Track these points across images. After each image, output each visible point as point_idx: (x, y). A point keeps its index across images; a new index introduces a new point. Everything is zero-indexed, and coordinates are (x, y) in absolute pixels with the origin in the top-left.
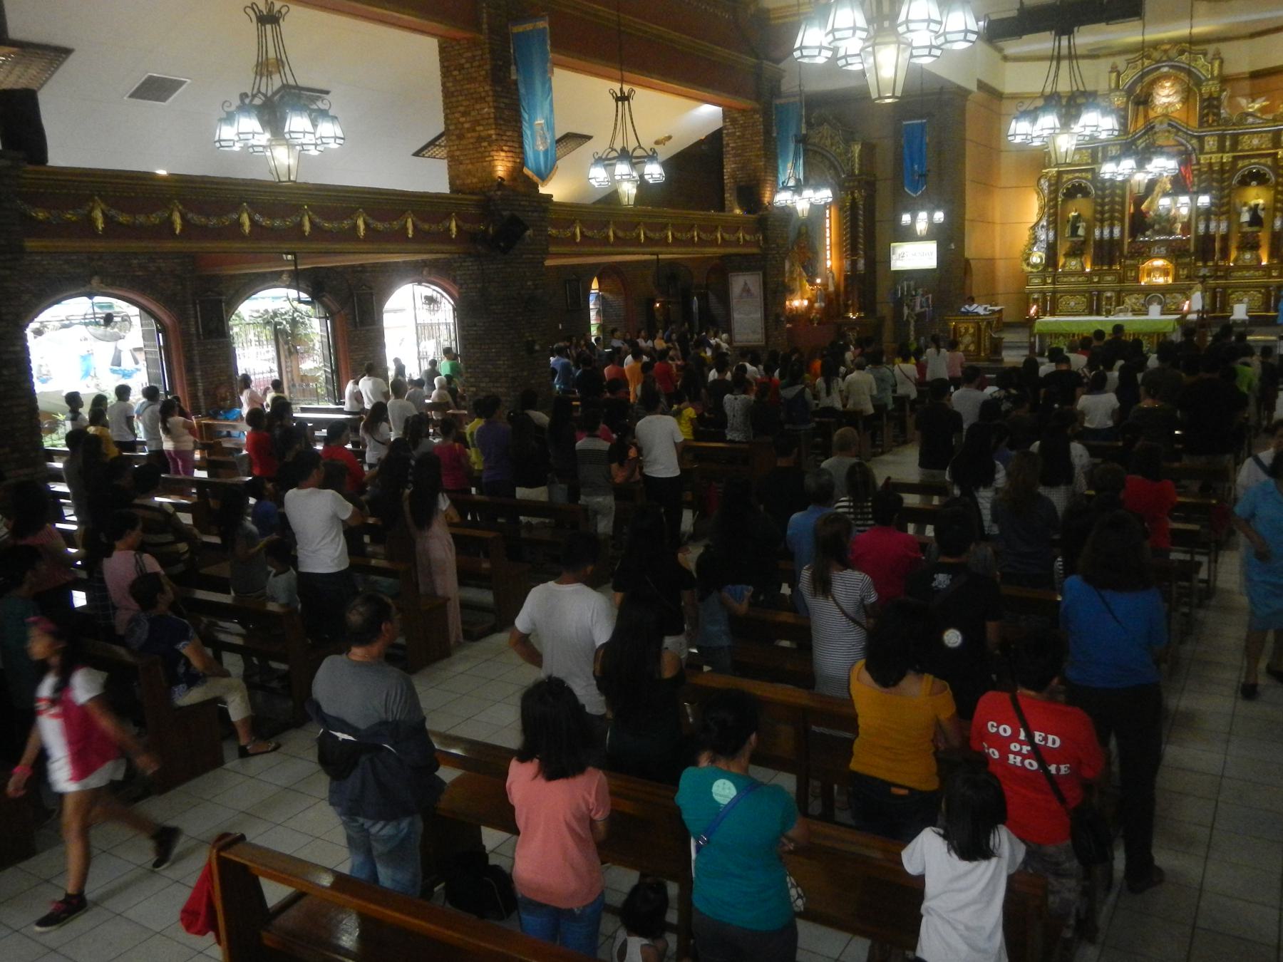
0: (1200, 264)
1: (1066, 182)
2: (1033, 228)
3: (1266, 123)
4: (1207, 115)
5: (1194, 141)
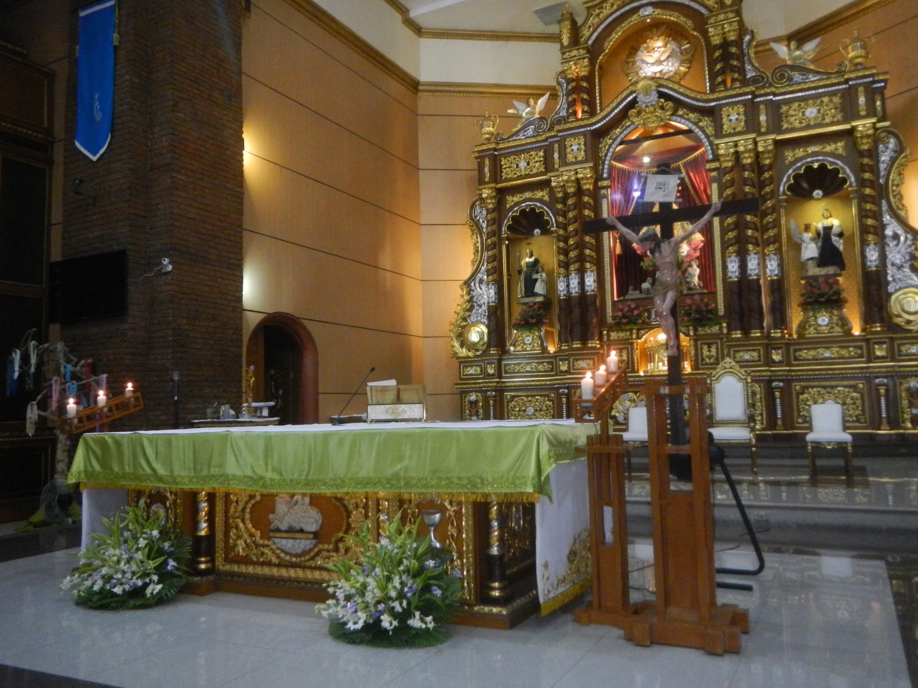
0: (738, 335)
1: (512, 208)
2: (467, 283)
3: (827, 79)
4: (723, 71)
5: (706, 122)
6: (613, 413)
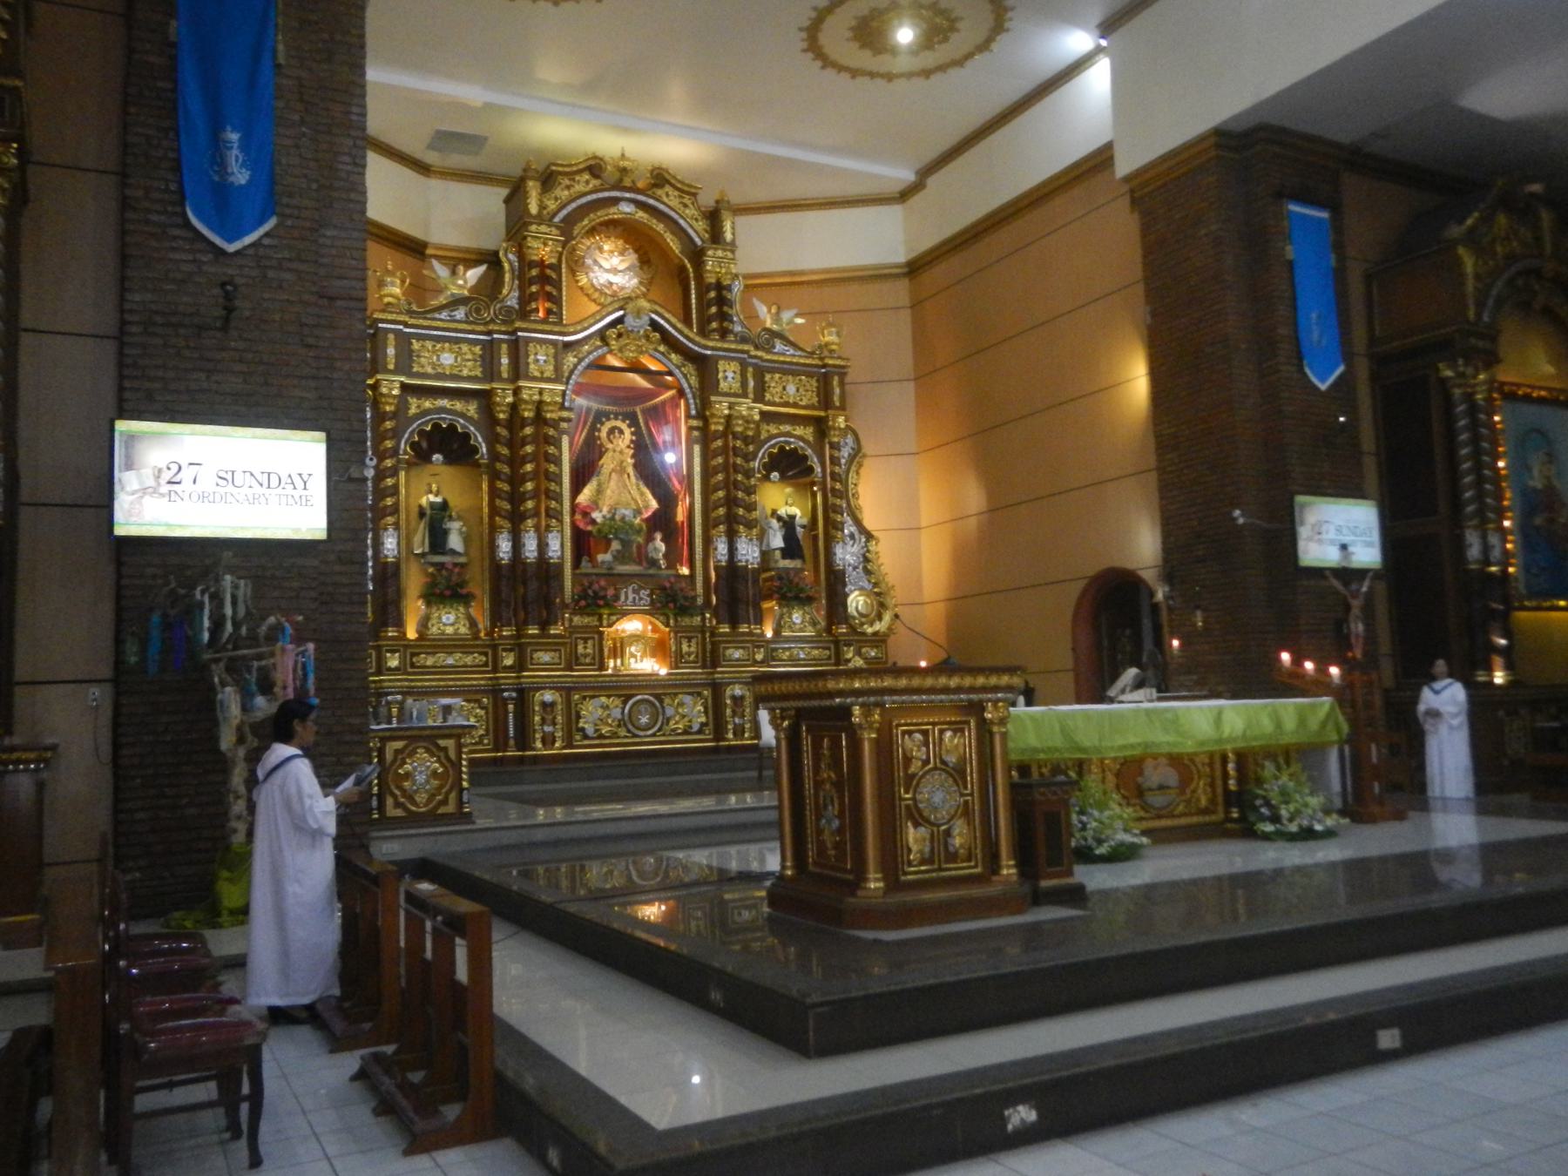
0: (725, 629)
5: (690, 369)
6: (581, 725)
